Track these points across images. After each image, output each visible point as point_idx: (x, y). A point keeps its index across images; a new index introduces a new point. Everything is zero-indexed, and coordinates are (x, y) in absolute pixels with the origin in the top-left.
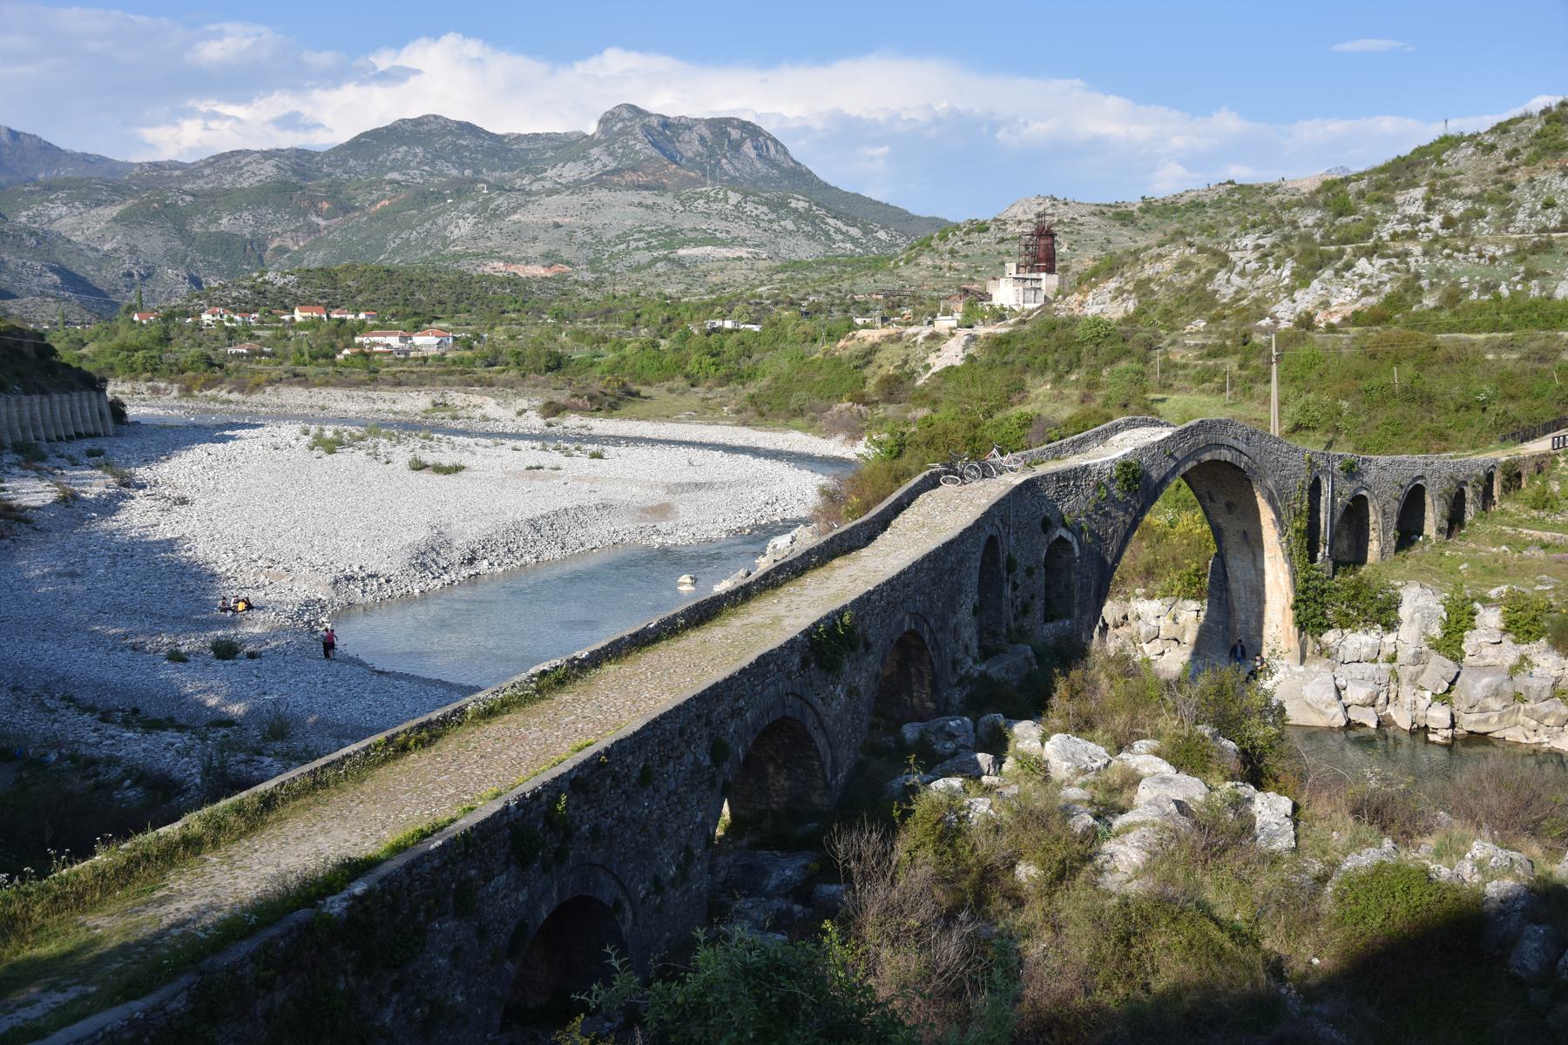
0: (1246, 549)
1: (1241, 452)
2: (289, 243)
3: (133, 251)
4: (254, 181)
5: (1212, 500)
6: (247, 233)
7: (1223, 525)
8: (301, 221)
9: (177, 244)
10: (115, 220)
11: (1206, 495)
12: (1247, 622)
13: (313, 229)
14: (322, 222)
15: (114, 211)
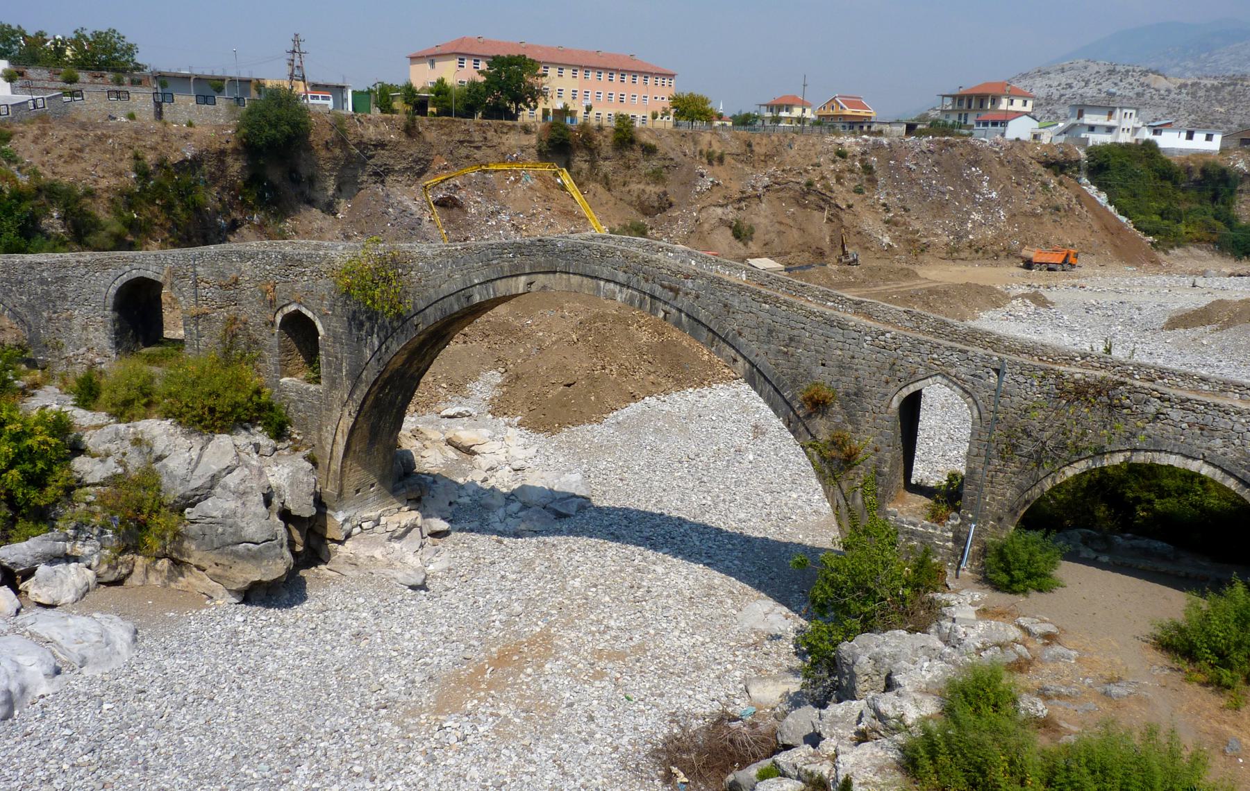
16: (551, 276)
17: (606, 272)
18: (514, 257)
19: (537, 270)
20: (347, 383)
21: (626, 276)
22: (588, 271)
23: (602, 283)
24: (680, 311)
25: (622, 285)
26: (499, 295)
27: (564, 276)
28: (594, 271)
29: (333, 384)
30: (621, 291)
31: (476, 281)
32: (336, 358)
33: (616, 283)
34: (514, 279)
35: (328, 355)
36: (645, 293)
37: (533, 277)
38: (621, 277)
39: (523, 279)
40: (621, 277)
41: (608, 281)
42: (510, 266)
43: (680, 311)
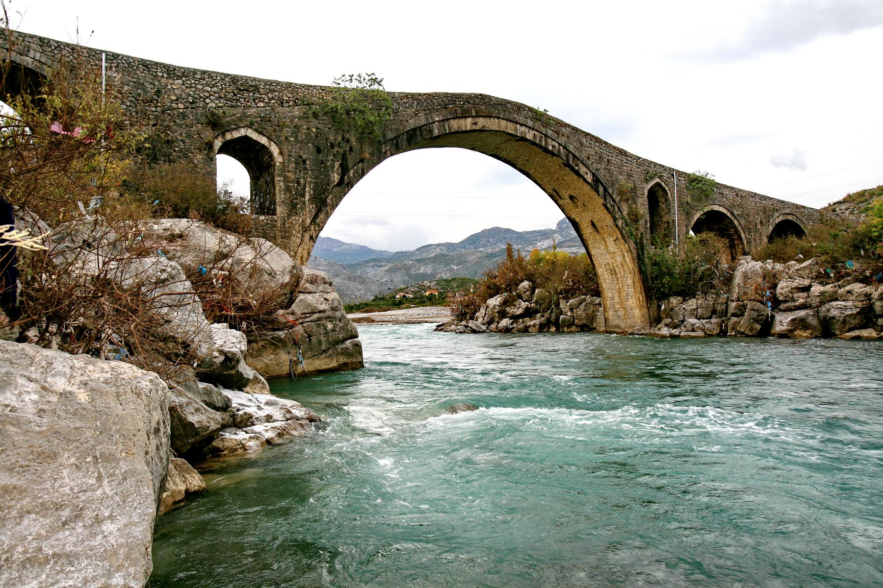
0: (598, 237)
1: (546, 136)
2: (444, 276)
3: (392, 281)
4: (433, 255)
5: (561, 198)
6: (429, 272)
7: (577, 220)
8: (448, 267)
9: (406, 278)
10: (386, 271)
11: (555, 194)
12: (613, 299)
13: (451, 270)
14: (455, 267)
15: (386, 268)
16: (488, 119)
17: (521, 119)
18: (464, 104)
19: (480, 114)
20: (310, 208)
21: (532, 123)
22: (511, 118)
23: (518, 126)
24: (560, 145)
25: (530, 128)
26: (452, 130)
27: (496, 120)
28: (514, 118)
29: (293, 208)
30: (529, 132)
31: (437, 119)
32: (298, 183)
33: (526, 126)
34: (464, 120)
35: (286, 180)
36: (542, 133)
37: (477, 120)
38: (530, 123)
39: (469, 120)
40: (530, 123)
41: (521, 125)
42: (462, 110)
43: (560, 145)
